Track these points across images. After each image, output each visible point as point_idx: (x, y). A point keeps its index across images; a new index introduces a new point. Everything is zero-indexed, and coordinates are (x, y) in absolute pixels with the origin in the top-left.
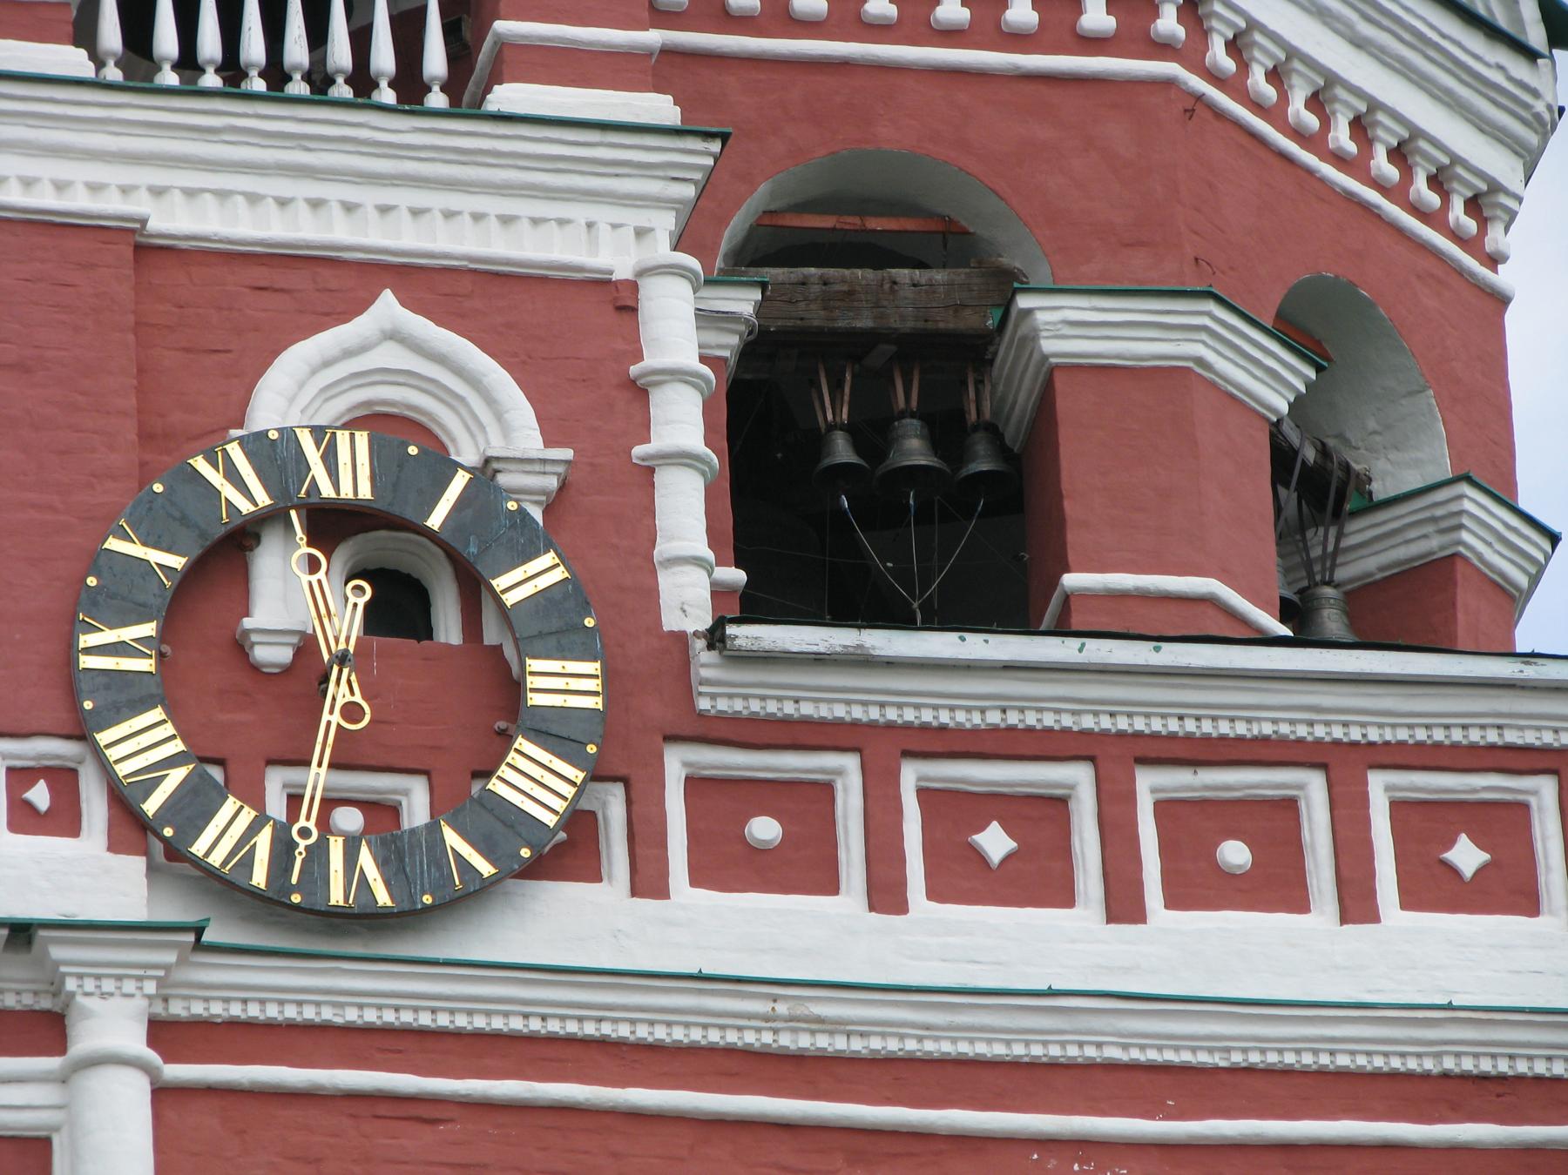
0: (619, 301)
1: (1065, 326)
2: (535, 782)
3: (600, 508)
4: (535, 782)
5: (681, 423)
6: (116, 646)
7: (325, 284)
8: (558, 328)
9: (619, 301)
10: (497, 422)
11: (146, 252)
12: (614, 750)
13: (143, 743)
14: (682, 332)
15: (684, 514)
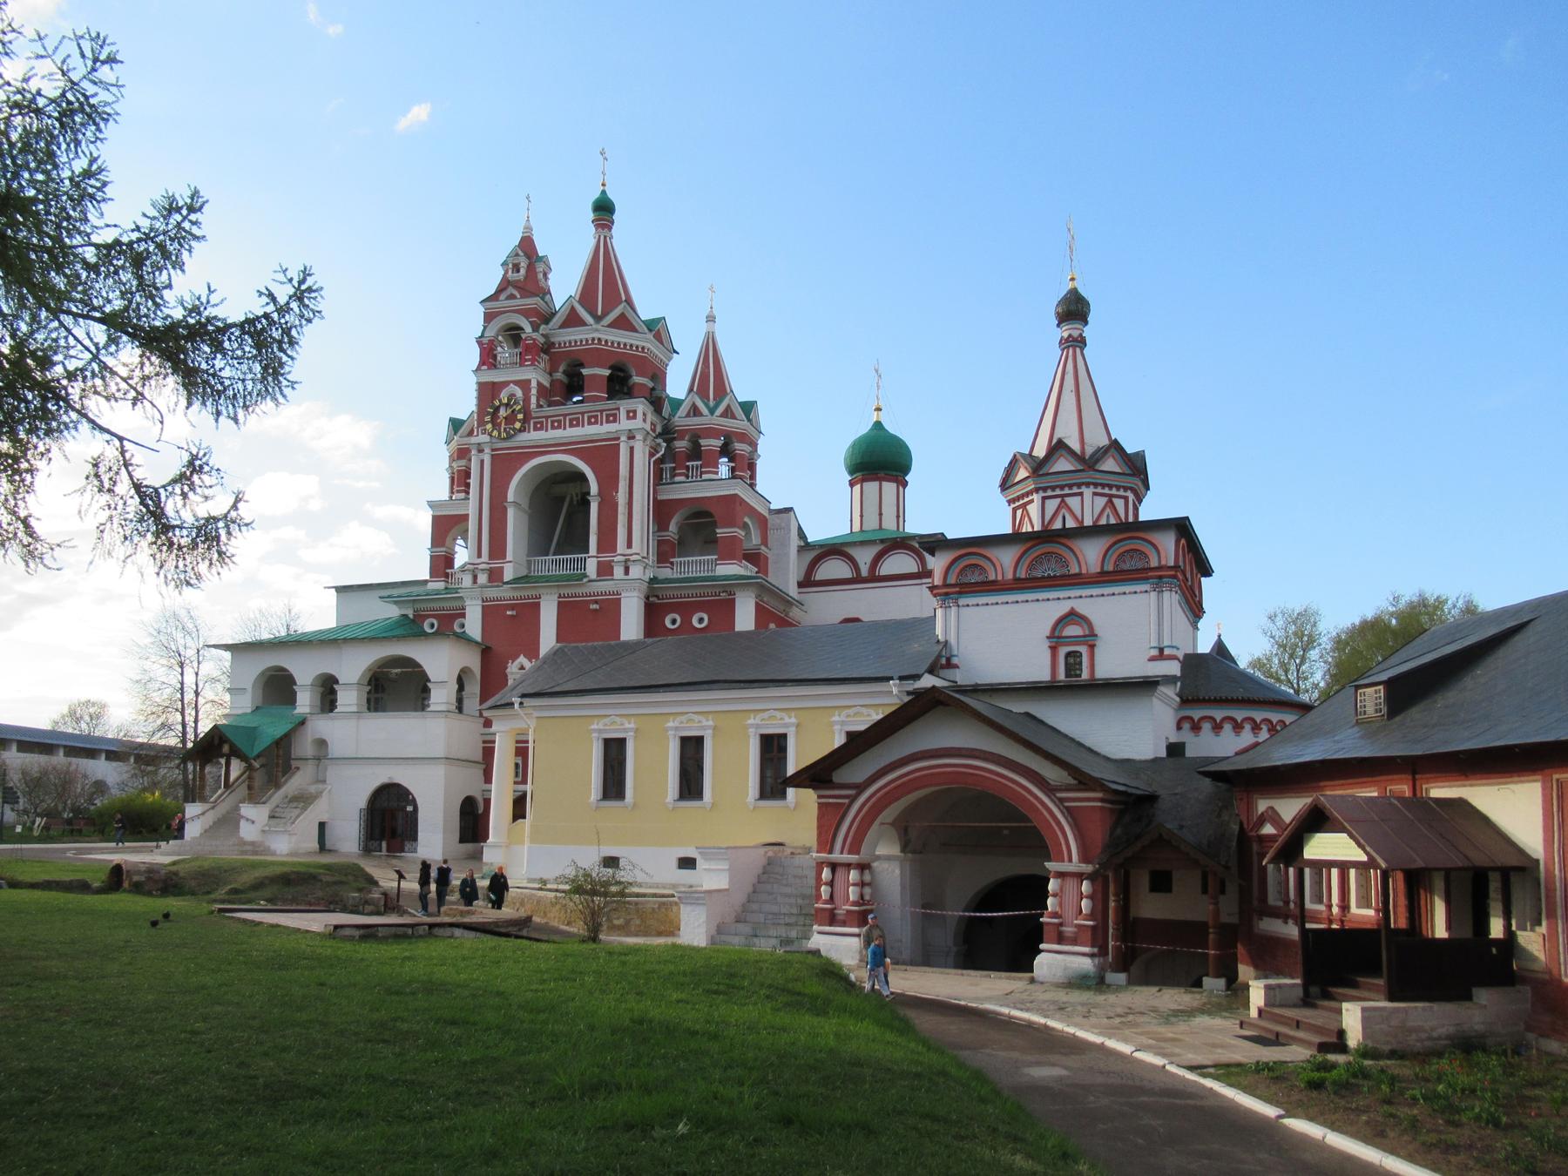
0: (529, 381)
1: (585, 372)
2: (518, 425)
3: (527, 399)
4: (518, 425)
5: (534, 391)
6: (488, 418)
7: (505, 384)
8: (524, 385)
9: (529, 381)
10: (519, 393)
11: (494, 384)
12: (525, 421)
13: (489, 426)
14: (534, 384)
15: (533, 400)
